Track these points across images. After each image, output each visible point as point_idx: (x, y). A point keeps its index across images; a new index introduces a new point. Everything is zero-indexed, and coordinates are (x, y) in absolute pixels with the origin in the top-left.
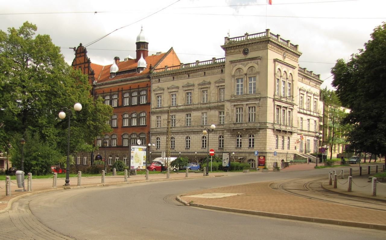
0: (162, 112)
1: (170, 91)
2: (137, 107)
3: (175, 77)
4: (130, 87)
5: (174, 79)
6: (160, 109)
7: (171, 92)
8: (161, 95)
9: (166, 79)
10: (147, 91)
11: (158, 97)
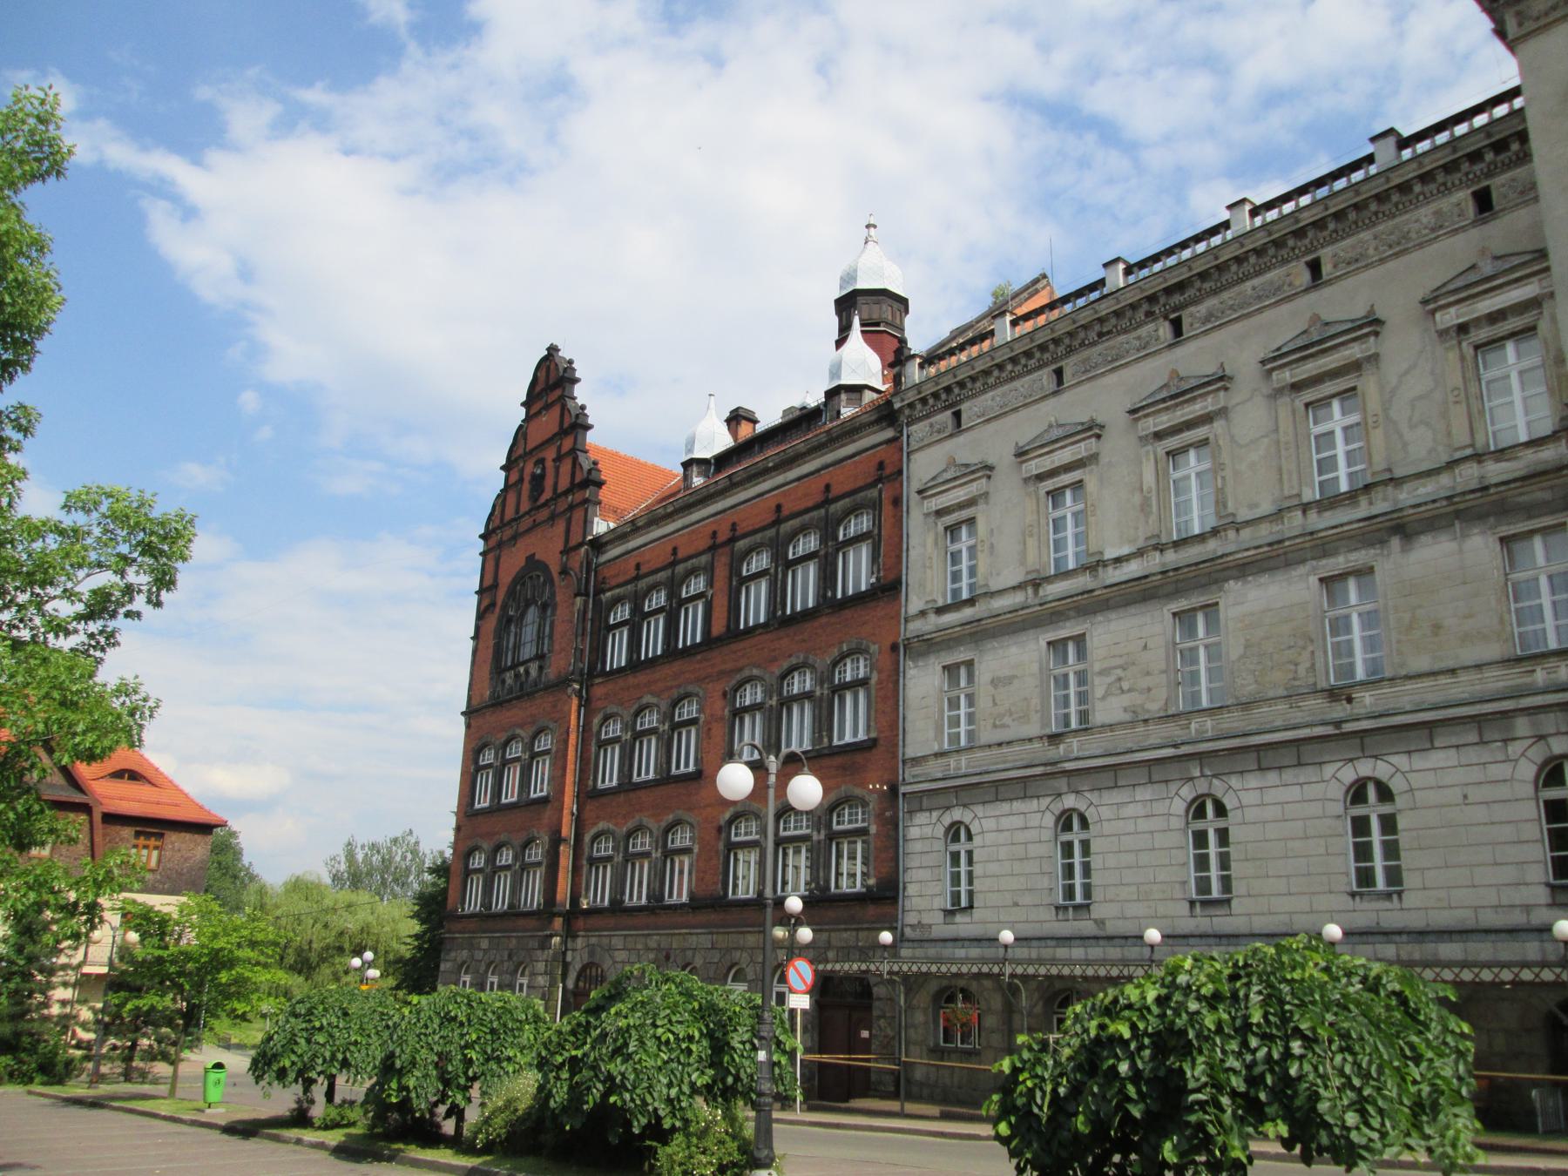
0: (981, 633)
1: (1034, 466)
2: (816, 624)
3: (1070, 366)
4: (779, 508)
5: (1060, 381)
6: (967, 613)
7: (1040, 477)
9: (1004, 395)
10: (875, 506)
11: (953, 530)
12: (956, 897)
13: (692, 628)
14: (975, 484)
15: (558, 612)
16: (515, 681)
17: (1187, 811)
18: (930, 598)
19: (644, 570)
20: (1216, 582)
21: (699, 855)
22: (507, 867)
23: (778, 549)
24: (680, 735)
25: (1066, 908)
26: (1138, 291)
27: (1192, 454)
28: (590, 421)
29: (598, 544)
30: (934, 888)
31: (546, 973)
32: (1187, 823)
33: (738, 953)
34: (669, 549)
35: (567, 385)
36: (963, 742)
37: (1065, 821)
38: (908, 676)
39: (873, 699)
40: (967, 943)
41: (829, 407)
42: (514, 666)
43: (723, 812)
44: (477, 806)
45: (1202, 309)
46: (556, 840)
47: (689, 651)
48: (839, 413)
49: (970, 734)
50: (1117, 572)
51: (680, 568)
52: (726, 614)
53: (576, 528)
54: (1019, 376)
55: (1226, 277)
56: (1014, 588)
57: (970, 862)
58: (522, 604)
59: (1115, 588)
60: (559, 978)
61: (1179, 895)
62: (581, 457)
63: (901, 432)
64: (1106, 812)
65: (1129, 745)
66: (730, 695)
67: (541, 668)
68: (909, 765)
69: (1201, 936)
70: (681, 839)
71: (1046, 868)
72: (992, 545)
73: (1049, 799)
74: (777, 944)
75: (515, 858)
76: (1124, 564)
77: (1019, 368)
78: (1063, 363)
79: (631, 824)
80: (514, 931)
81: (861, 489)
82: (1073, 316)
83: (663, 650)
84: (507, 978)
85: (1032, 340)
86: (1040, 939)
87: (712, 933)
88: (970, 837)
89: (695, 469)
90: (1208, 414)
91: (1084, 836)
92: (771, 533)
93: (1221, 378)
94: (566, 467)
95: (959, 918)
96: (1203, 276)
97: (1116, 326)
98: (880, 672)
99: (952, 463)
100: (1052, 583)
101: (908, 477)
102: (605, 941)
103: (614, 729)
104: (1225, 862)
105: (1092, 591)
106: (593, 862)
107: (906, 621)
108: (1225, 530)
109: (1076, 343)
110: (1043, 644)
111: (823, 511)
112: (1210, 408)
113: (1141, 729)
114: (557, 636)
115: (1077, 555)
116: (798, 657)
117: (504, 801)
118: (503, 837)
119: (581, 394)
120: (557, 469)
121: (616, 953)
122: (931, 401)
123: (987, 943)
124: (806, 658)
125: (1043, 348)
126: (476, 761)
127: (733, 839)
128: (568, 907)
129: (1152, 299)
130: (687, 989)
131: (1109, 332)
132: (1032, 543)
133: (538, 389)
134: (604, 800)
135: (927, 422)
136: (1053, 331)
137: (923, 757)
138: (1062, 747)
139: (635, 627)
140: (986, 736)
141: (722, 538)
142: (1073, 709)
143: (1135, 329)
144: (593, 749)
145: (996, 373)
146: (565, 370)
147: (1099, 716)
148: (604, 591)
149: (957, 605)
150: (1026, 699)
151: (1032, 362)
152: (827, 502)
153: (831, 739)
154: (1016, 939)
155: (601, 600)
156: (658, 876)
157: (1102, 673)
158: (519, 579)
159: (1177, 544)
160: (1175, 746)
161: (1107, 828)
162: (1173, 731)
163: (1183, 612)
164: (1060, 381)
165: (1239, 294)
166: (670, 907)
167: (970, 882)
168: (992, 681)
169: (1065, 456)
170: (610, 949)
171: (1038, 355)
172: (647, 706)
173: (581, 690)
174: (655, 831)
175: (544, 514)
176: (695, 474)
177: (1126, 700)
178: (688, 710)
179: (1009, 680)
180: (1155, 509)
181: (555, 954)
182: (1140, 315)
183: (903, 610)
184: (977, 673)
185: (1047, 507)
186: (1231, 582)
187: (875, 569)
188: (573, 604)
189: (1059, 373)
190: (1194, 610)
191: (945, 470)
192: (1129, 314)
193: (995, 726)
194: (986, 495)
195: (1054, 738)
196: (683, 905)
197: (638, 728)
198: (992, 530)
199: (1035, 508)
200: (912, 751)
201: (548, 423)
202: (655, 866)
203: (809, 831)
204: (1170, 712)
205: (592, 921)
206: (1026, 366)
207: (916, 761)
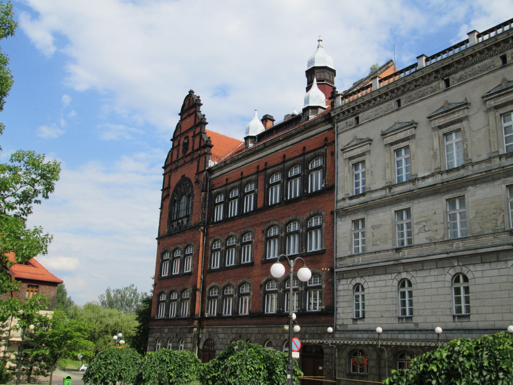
0: (367, 207)
2: (300, 203)
3: (403, 99)
5: (399, 105)
6: (362, 199)
7: (392, 144)
8: (360, 159)
9: (376, 111)
10: (324, 156)
11: (356, 165)
12: (357, 314)
13: (249, 205)
14: (365, 147)
15: (195, 198)
16: (178, 226)
17: (452, 280)
18: (346, 193)
19: (229, 181)
20: (464, 187)
21: (253, 296)
22: (175, 300)
23: (284, 172)
24: (245, 248)
25: (402, 318)
26: (431, 68)
27: (454, 135)
28: (207, 121)
29: (211, 171)
30: (348, 310)
31: (191, 342)
32: (452, 284)
33: (269, 335)
34: (240, 173)
35: (197, 106)
36: (360, 251)
37: (402, 283)
38: (338, 225)
39: (324, 234)
40: (362, 332)
41: (305, 115)
42: (177, 220)
43: (263, 279)
44: (163, 276)
45: (457, 76)
46: (195, 290)
47: (248, 214)
48: (308, 117)
49: (363, 248)
50: (423, 183)
51: (244, 181)
52: (263, 199)
53: (202, 165)
54: (382, 103)
55: (468, 63)
56: (381, 189)
57: (363, 299)
58: (180, 195)
59: (422, 189)
60: (196, 344)
61: (448, 312)
62: (203, 136)
63: (334, 126)
64: (419, 280)
65: (428, 253)
66: (265, 232)
67: (188, 221)
68: (338, 260)
69: (457, 330)
70: (246, 289)
71: (394, 302)
72: (372, 171)
73: (395, 275)
74: (285, 332)
75: (178, 296)
76: (426, 179)
77: (383, 99)
78: (400, 98)
79: (225, 283)
80: (178, 326)
81: (318, 149)
82: (404, 78)
83: (237, 213)
84: (175, 344)
85: (388, 89)
86: (392, 330)
87: (258, 327)
88: (363, 289)
89: (250, 140)
90: (460, 118)
91: (410, 289)
92: (282, 166)
93: (466, 104)
94: (197, 139)
95: (359, 322)
96: (458, 62)
97: (422, 83)
98: (326, 223)
99: (355, 138)
100: (396, 187)
101: (337, 144)
102: (215, 330)
103: (218, 245)
104: (467, 300)
105: (413, 190)
106: (210, 298)
107: (337, 202)
108: (467, 166)
109: (406, 90)
110: (393, 212)
111: (302, 158)
112: (461, 116)
113: (433, 246)
114: (194, 208)
115: (407, 175)
116: (293, 217)
117: (173, 274)
118: (173, 288)
119: (203, 110)
120: (194, 141)
121: (219, 335)
122: (346, 113)
123: (370, 332)
124: (296, 217)
125: (392, 91)
126: (162, 257)
127: (267, 290)
128: (200, 316)
129: (437, 71)
130: (258, 350)
131: (419, 85)
132: (388, 171)
133: (185, 108)
134: (213, 274)
135: (345, 122)
136: (396, 85)
137: (344, 257)
138: (401, 253)
139: (226, 204)
140: (369, 249)
141: (261, 168)
142: (405, 238)
143: (430, 84)
144: (209, 253)
145: (373, 102)
146: (196, 100)
147: (416, 241)
148: (213, 190)
149: (358, 196)
150: (386, 234)
151: (388, 97)
152: (304, 154)
153: (306, 250)
154: (383, 331)
155: (212, 193)
156: (236, 304)
157: (417, 223)
158: (179, 185)
159: (448, 172)
160: (447, 253)
161: (419, 286)
162: (446, 247)
163: (451, 199)
164: (399, 105)
165: (473, 69)
166: (241, 317)
167: (363, 308)
168: (372, 227)
169: (401, 135)
170: (217, 333)
171: (390, 94)
172: (231, 236)
173: (204, 229)
174: (235, 286)
175: (188, 159)
176: (249, 142)
177: (427, 235)
178: (248, 238)
179: (379, 226)
180: (438, 157)
181: (194, 335)
182: (432, 78)
183: (336, 198)
184: (366, 223)
185: (394, 156)
186: (470, 187)
187: (324, 181)
188: (201, 195)
189: (399, 102)
190: (455, 198)
191: (352, 141)
192: (427, 78)
193: (373, 245)
194: (369, 151)
195: (398, 250)
196: (247, 316)
197: (228, 245)
198: (372, 165)
199: (389, 156)
200: (339, 255)
201: (190, 122)
202: (235, 301)
203: (297, 287)
204: (445, 239)
205: (210, 322)
206: (385, 99)
207: (341, 259)
